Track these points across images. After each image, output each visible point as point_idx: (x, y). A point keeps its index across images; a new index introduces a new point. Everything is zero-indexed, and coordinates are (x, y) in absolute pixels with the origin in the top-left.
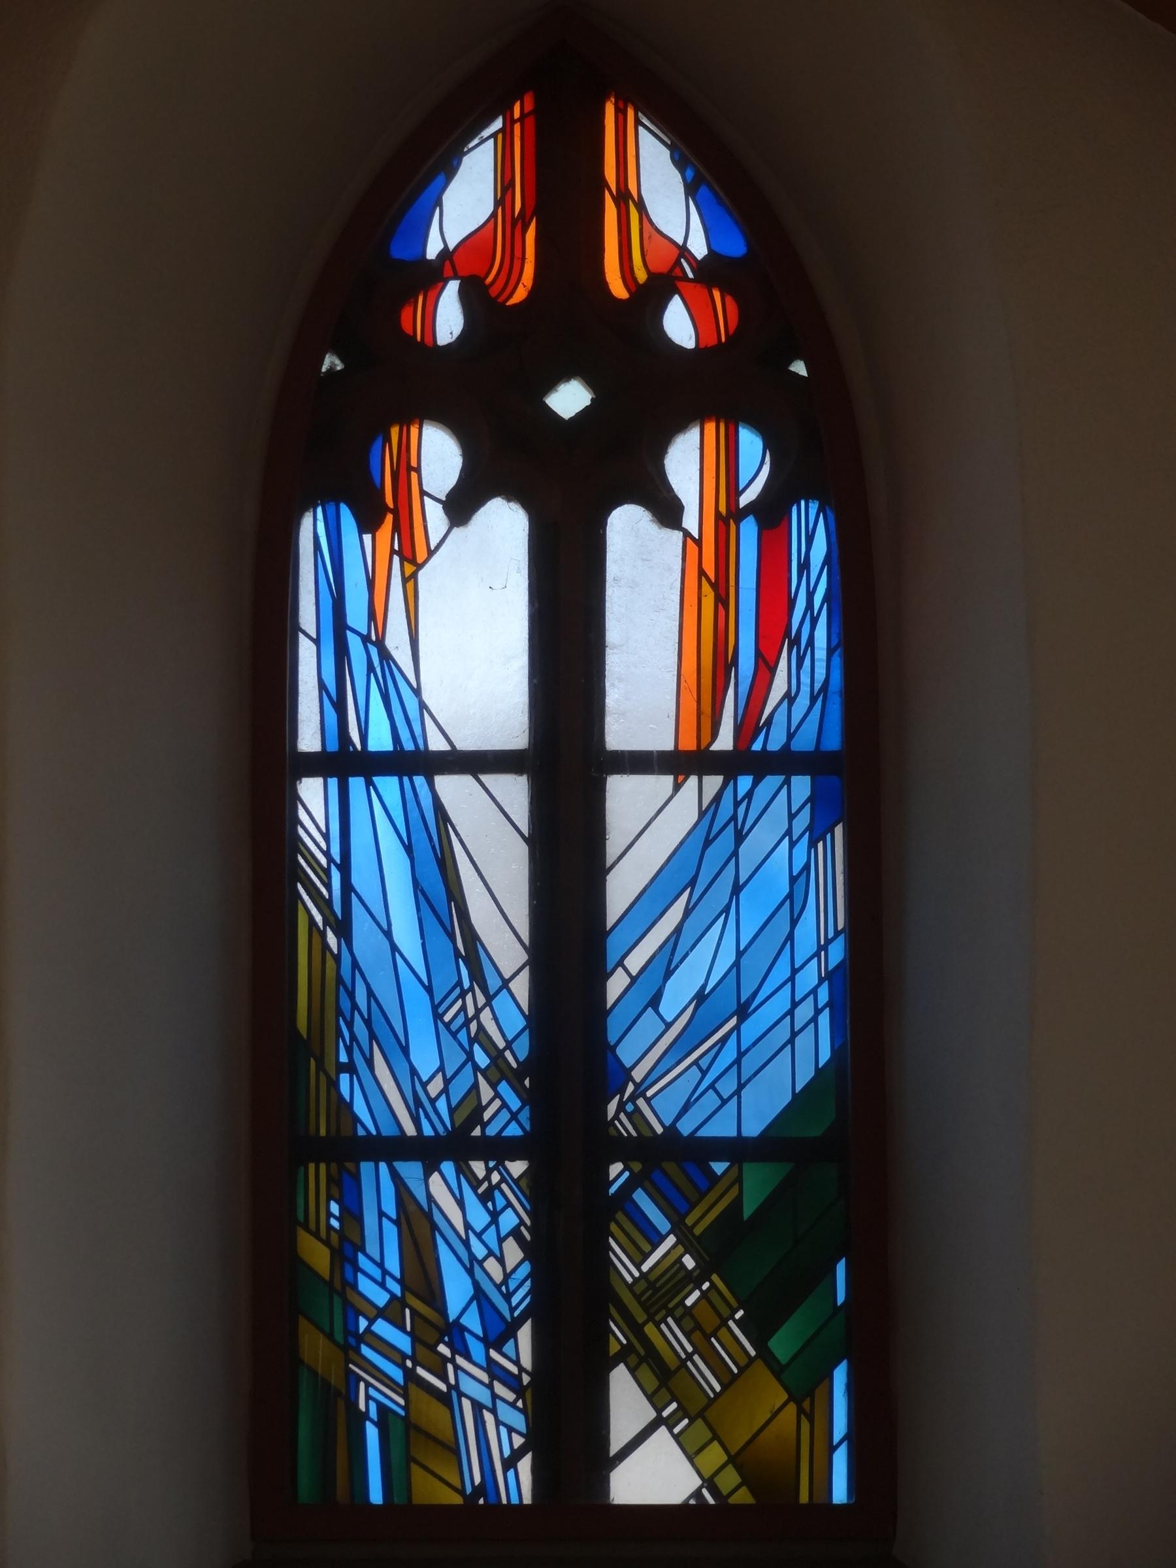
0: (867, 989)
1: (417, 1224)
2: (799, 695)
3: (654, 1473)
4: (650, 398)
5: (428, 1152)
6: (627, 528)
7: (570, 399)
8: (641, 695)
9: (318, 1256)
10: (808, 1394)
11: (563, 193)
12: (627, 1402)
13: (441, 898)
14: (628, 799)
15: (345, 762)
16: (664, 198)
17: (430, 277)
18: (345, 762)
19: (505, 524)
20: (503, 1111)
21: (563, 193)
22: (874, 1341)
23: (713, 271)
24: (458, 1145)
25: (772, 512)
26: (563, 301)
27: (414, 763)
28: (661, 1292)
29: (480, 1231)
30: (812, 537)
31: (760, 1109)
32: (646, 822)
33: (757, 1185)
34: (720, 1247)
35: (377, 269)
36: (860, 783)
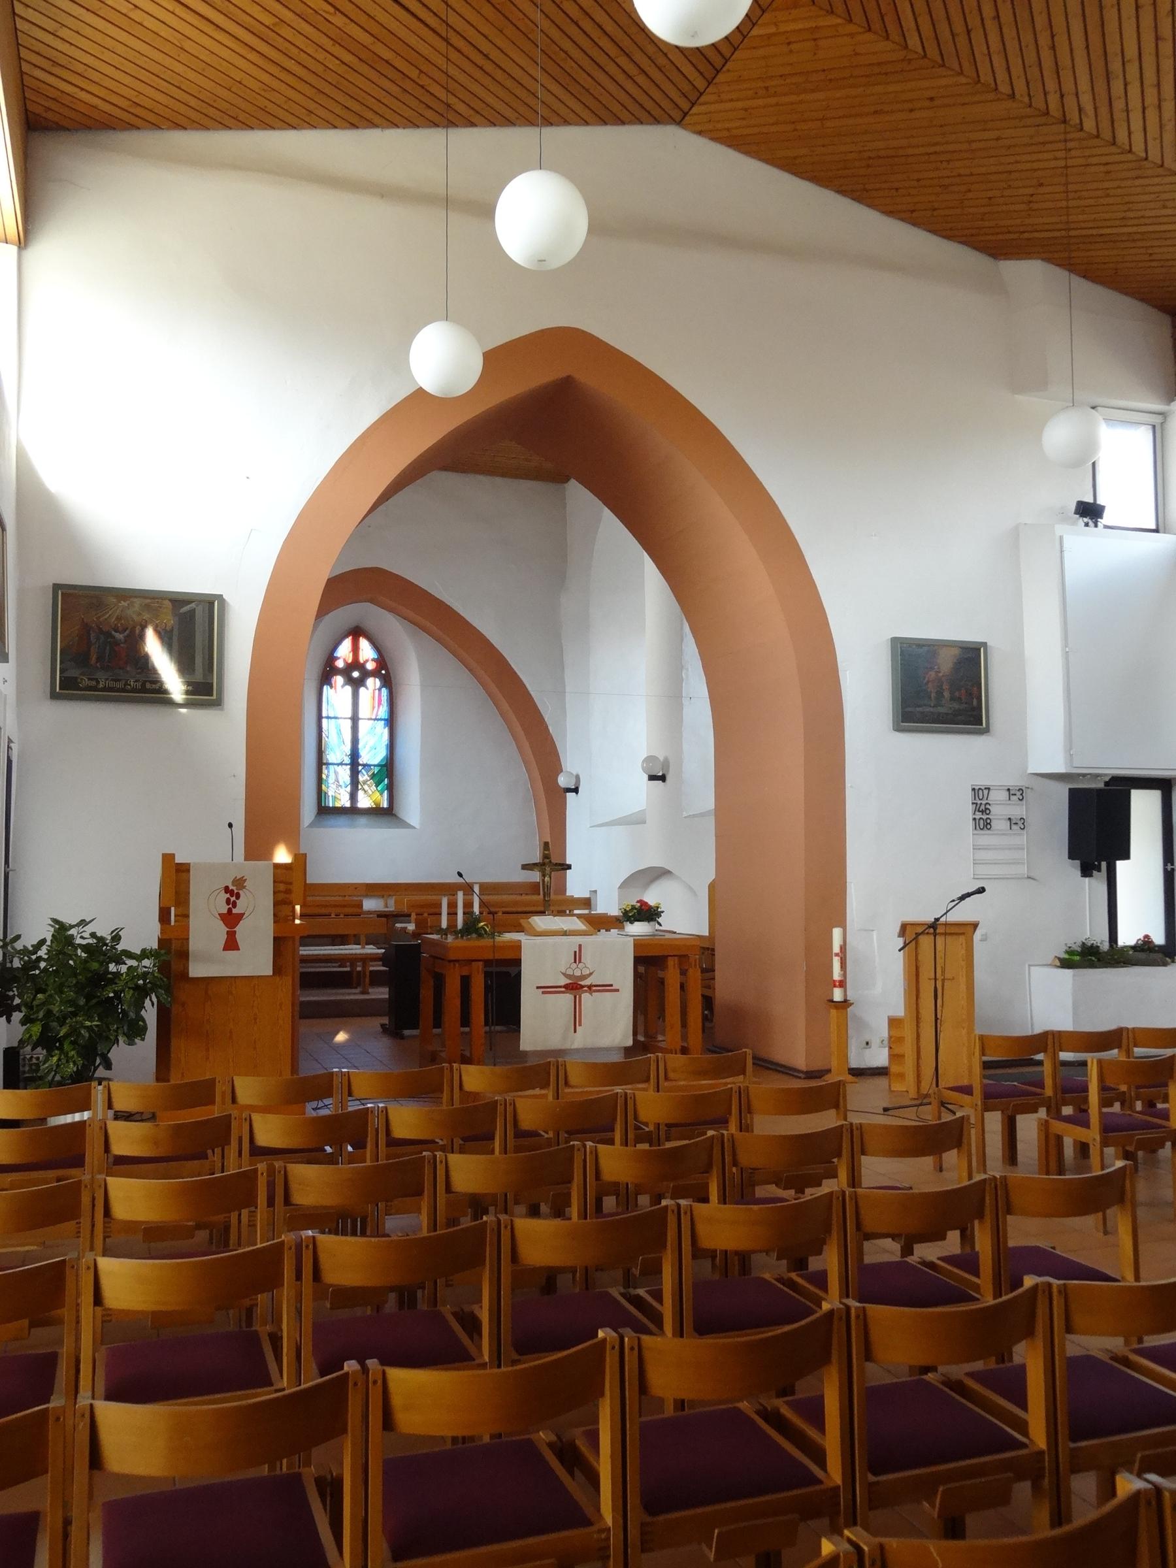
0: (391, 746)
1: (336, 773)
2: (383, 712)
3: (364, 802)
4: (366, 674)
5: (338, 765)
6: (362, 690)
7: (356, 674)
8: (365, 710)
9: (324, 776)
10: (381, 794)
11: (355, 649)
12: (360, 794)
13: (339, 733)
14: (361, 723)
15: (328, 718)
16: (367, 652)
17: (337, 658)
18: (328, 718)
19: (348, 689)
20: (347, 760)
21: (355, 649)
22: (391, 788)
23: (373, 660)
24: (341, 764)
25: (380, 690)
26: (356, 664)
27: (336, 718)
28: (365, 782)
29: (345, 774)
30: (384, 691)
31: (376, 762)
32: (363, 725)
33: (376, 770)
34: (373, 776)
35: (331, 659)
36: (391, 722)
